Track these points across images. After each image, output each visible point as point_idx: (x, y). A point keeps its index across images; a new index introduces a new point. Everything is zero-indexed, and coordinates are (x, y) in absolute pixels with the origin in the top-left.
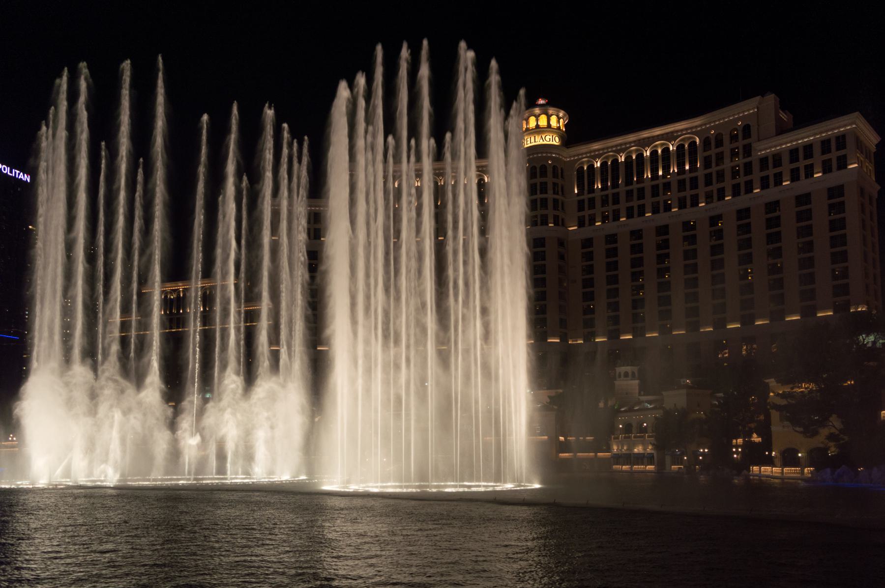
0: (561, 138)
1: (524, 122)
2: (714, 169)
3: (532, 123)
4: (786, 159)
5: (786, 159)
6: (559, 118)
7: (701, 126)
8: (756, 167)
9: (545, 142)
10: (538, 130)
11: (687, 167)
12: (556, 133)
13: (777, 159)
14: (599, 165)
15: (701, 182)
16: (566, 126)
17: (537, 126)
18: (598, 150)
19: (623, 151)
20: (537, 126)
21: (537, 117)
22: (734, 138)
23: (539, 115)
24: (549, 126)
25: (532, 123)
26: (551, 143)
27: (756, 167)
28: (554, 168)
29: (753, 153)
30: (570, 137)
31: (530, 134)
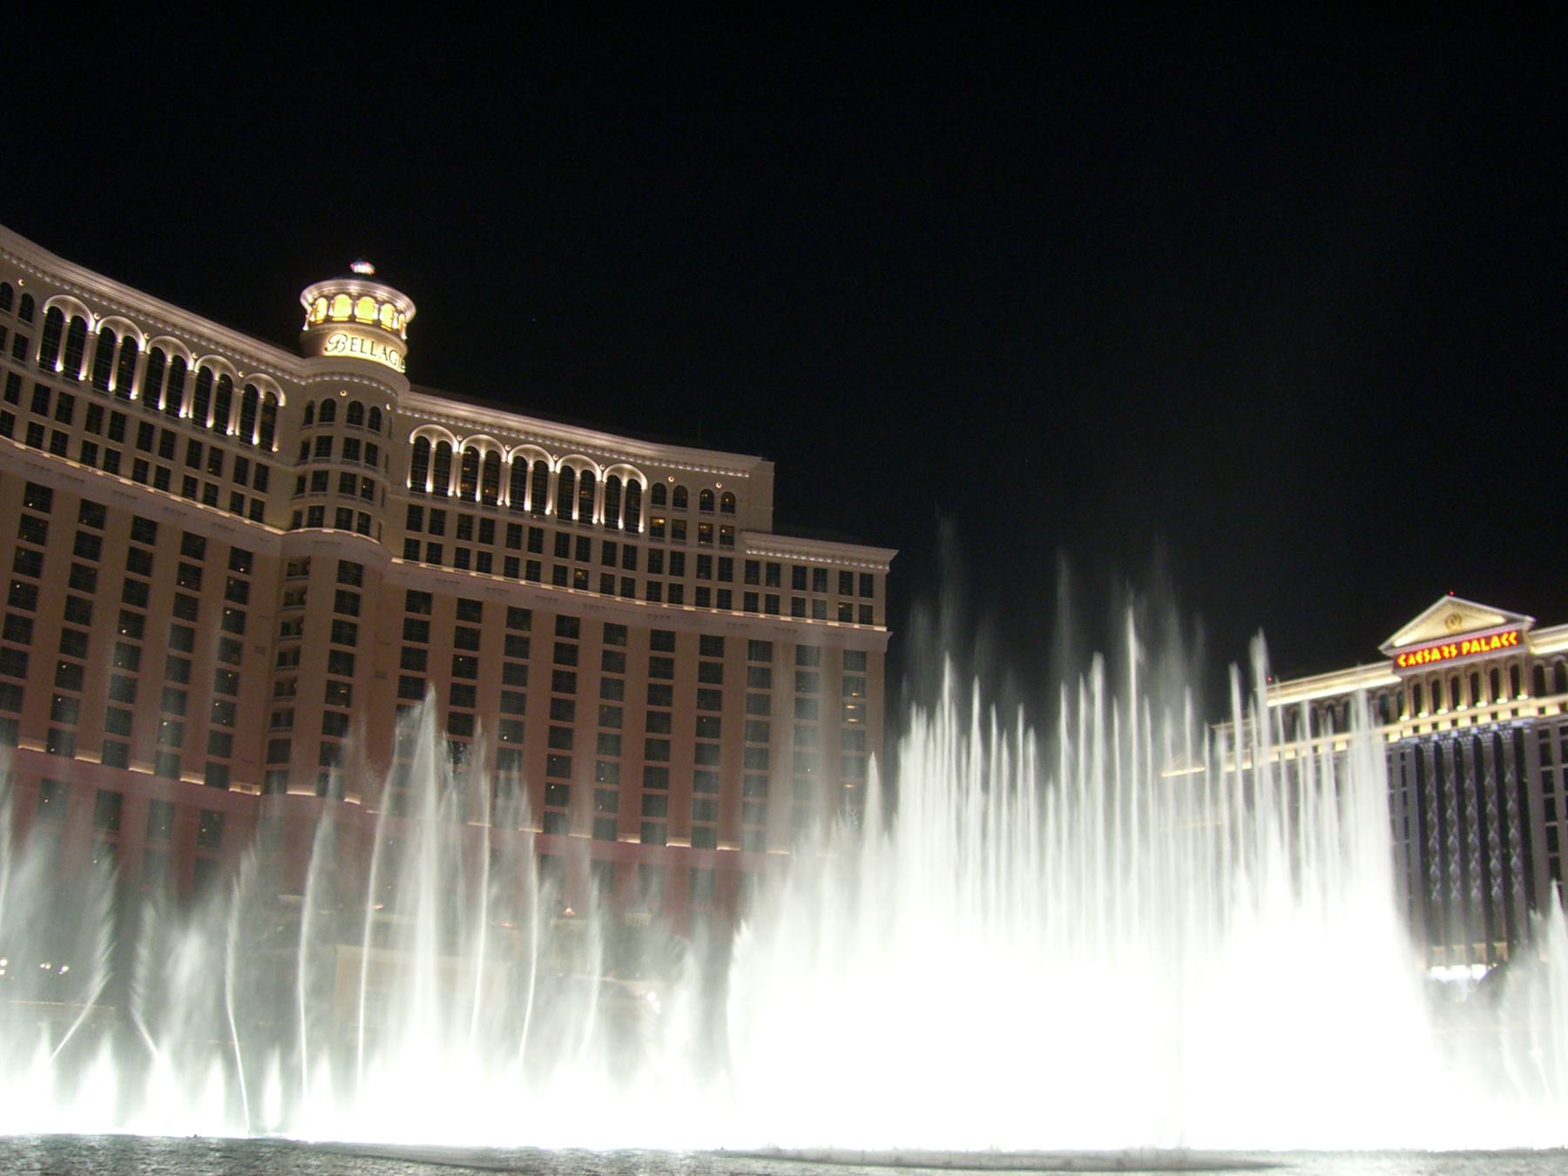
2: (668, 546)
3: (366, 311)
4: (786, 577)
5: (786, 577)
7: (651, 459)
8: (739, 571)
9: (388, 364)
10: (375, 329)
13: (774, 569)
14: (511, 461)
15: (643, 560)
17: (377, 324)
18: (466, 420)
19: (513, 443)
22: (707, 503)
25: (366, 311)
27: (739, 571)
29: (737, 545)
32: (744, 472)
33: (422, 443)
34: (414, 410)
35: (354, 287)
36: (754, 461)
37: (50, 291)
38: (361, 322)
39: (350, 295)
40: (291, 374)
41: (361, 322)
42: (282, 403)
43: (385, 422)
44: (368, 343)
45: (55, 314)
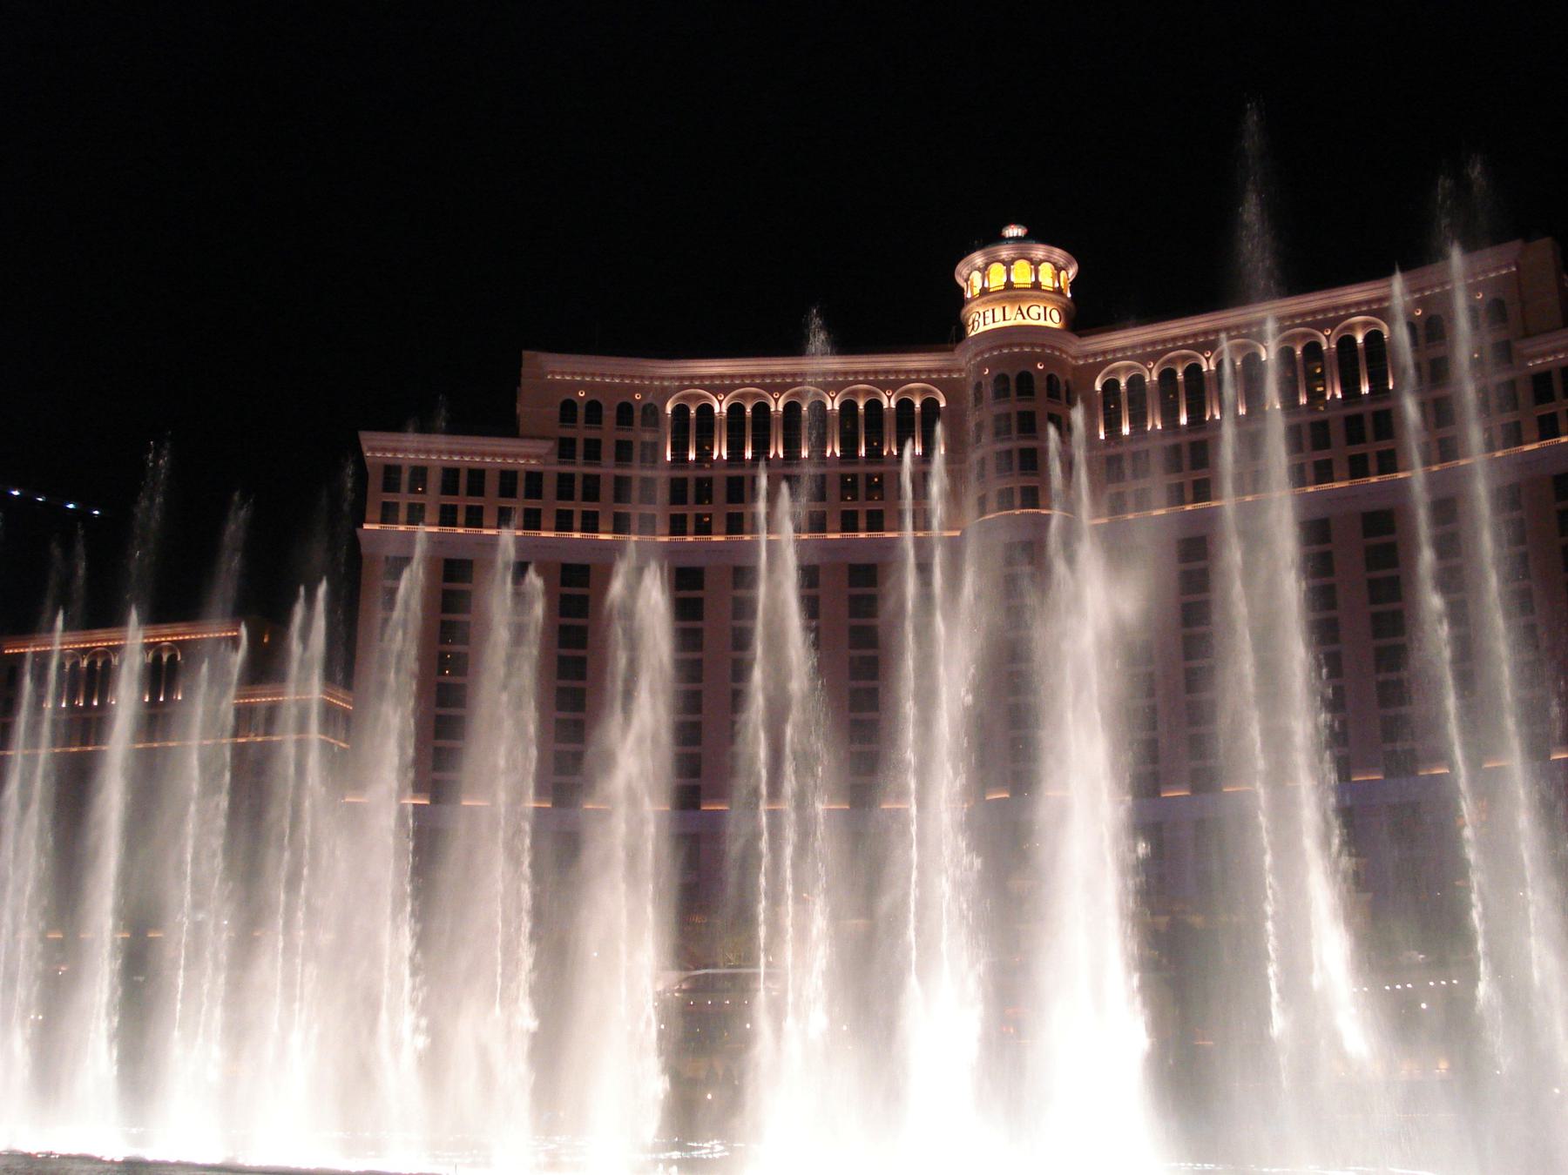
0: (1066, 314)
1: (976, 277)
3: (997, 276)
6: (1058, 269)
9: (1028, 322)
10: (1010, 292)
11: (1365, 389)
12: (1053, 301)
16: (1074, 285)
17: (1009, 285)
20: (1009, 285)
21: (1008, 265)
23: (1012, 262)
24: (1036, 285)
25: (997, 276)
26: (1041, 322)
28: (1050, 378)
30: (1089, 309)
31: (996, 300)
32: (1508, 266)
33: (1111, 386)
34: (1095, 355)
35: (1005, 252)
36: (1517, 244)
37: (665, 394)
38: (1013, 287)
39: (1031, 261)
40: (950, 371)
41: (1013, 287)
42: (943, 404)
43: (1040, 385)
44: (999, 313)
45: (681, 411)
